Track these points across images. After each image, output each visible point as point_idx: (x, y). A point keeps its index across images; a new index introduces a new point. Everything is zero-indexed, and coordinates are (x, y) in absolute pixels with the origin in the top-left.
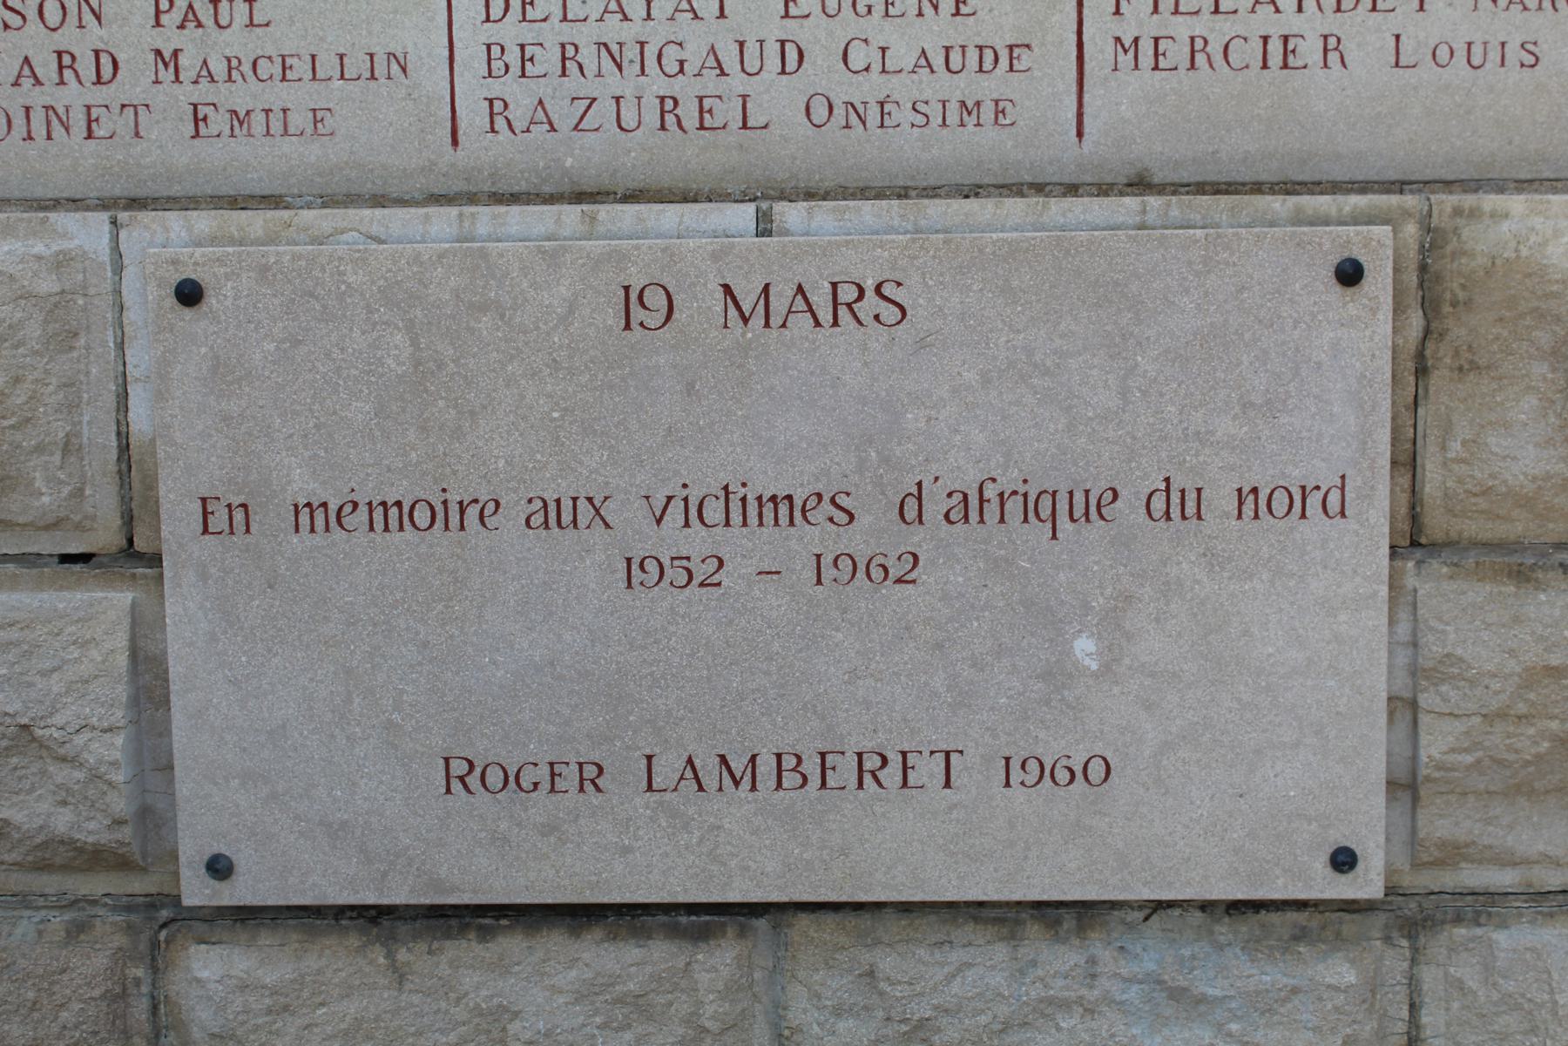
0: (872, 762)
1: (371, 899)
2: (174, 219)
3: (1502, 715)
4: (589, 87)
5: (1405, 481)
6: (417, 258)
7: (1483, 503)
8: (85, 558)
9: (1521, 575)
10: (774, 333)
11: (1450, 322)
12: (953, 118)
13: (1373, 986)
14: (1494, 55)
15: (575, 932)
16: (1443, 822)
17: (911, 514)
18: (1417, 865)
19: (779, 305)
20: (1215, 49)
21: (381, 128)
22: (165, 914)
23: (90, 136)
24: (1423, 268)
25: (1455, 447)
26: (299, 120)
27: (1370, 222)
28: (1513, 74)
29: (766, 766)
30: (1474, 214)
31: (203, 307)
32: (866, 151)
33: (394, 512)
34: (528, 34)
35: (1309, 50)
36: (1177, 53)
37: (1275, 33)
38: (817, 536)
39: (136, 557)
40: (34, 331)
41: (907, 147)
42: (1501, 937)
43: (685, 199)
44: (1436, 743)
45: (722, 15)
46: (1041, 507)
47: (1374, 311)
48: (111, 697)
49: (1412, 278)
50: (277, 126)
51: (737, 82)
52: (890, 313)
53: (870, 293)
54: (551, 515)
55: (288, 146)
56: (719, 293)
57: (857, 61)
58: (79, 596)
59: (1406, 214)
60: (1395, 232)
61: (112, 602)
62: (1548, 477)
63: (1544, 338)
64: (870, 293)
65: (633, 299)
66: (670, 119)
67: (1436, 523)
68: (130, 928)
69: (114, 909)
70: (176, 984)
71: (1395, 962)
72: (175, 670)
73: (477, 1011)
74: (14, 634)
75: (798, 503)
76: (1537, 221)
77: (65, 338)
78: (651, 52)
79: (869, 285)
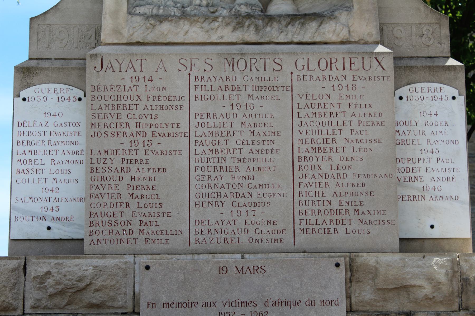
2: (145, 256)
5: (349, 300)
6: (186, 262)
7: (362, 304)
8: (125, 313)
10: (244, 274)
11: (355, 274)
12: (273, 242)
14: (362, 232)
17: (266, 305)
19: (245, 270)
21: (176, 242)
24: (350, 265)
25: (357, 294)
26: (163, 241)
27: (341, 257)
28: (366, 235)
30: (358, 256)
32: (258, 246)
34: (202, 227)
35: (332, 231)
36: (310, 231)
37: (326, 228)
38: (251, 308)
40: (121, 274)
41: (265, 246)
43: (228, 254)
45: (235, 224)
46: (288, 304)
47: (342, 271)
49: (348, 266)
50: (159, 242)
51: (237, 235)
52: (263, 271)
54: (206, 305)
55: (162, 245)
56: (235, 268)
57: (257, 232)
59: (347, 256)
60: (345, 259)
62: (372, 299)
64: (260, 268)
65: (221, 269)
66: (226, 241)
67: (354, 307)
75: (248, 303)
76: (368, 257)
77: (125, 276)
78: (223, 230)
79: (260, 267)
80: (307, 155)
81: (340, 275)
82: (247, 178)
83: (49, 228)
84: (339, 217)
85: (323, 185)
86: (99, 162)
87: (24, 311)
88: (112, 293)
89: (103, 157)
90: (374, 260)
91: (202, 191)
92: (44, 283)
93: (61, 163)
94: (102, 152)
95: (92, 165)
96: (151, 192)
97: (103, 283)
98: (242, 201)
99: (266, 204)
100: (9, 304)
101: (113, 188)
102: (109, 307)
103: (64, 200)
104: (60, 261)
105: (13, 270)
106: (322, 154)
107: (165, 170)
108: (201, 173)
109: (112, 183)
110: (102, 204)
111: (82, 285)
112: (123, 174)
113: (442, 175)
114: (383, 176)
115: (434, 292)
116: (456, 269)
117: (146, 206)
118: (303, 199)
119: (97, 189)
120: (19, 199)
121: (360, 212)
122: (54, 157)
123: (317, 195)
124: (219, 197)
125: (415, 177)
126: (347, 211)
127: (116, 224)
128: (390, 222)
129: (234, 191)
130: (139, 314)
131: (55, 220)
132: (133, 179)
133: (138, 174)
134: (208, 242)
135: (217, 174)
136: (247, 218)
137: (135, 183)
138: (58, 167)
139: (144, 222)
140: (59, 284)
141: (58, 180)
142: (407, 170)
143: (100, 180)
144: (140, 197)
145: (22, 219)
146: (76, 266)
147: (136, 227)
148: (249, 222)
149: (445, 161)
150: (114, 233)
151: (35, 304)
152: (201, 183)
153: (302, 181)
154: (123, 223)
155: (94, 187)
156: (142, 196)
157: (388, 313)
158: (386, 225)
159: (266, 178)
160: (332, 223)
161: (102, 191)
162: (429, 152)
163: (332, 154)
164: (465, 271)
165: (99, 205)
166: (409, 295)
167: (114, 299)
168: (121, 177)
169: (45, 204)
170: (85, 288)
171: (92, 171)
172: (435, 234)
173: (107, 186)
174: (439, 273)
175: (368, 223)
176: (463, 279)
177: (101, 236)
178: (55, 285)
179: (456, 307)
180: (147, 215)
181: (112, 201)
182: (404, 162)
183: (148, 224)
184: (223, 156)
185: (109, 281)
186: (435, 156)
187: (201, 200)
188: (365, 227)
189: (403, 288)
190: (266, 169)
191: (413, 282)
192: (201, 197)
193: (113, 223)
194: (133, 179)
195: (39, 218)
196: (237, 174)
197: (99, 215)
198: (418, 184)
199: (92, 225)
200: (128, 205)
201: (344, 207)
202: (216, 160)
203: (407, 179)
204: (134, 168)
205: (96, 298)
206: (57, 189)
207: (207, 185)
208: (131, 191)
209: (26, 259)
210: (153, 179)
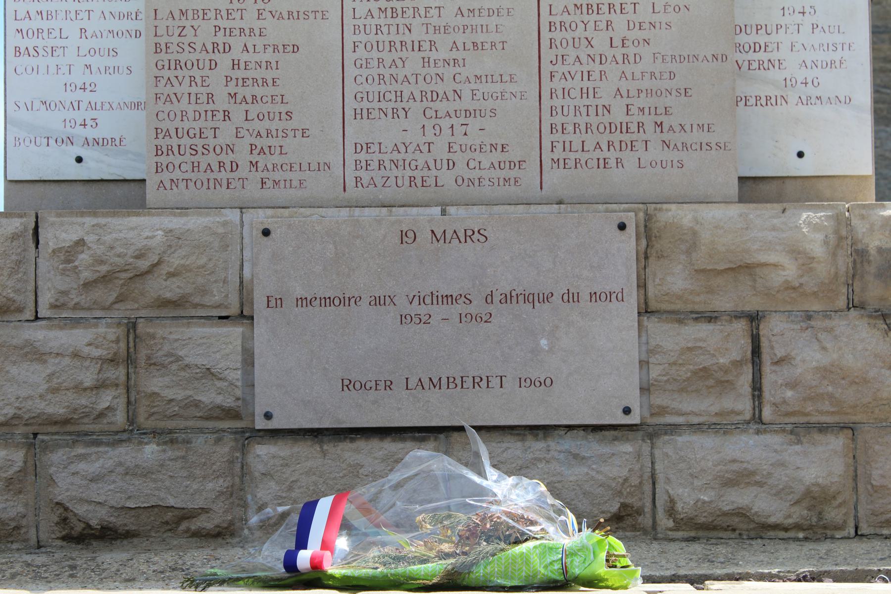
0: (477, 380)
1: (316, 426)
3: (675, 364)
4: (388, 173)
5: (642, 292)
6: (337, 222)
7: (666, 298)
8: (226, 318)
9: (680, 322)
10: (447, 245)
11: (654, 243)
12: (501, 183)
13: (639, 455)
14: (669, 164)
15: (382, 439)
16: (658, 400)
18: (652, 415)
19: (448, 236)
20: (583, 162)
22: (247, 435)
23: (228, 188)
24: (646, 226)
25: (657, 281)
26: (295, 183)
29: (444, 381)
30: (660, 210)
31: (270, 237)
33: (328, 300)
34: (368, 157)
35: (612, 163)
36: (571, 163)
37: (602, 157)
38: (460, 308)
39: (245, 317)
42: (679, 439)
43: (417, 206)
44: (655, 372)
45: (429, 151)
46: (529, 298)
47: (630, 238)
48: (236, 360)
49: (642, 229)
50: (288, 185)
51: (434, 172)
52: (482, 239)
53: (476, 233)
54: (377, 301)
57: (472, 165)
58: (225, 330)
59: (640, 210)
60: (636, 215)
61: (235, 332)
62: (686, 290)
63: (683, 247)
64: (476, 233)
65: (403, 235)
66: (413, 183)
67: (653, 305)
68: (236, 440)
69: (231, 433)
70: (250, 458)
71: (646, 448)
72: (256, 351)
73: (350, 465)
74: (205, 341)
75: (454, 297)
76: (680, 212)
79: (476, 230)
80: (566, 18)
81: (627, 246)
82: (452, 63)
83: (79, 160)
84: (626, 138)
85: (596, 75)
86: (170, 34)
87: (37, 312)
88: (200, 280)
89: (177, 23)
90: (690, 217)
91: (368, 88)
92: (73, 261)
93: (99, 35)
94: (177, 14)
95: (158, 40)
96: (270, 90)
97: (182, 262)
98: (442, 107)
99: (489, 113)
100: (9, 299)
101: (199, 84)
102: (196, 306)
103: (107, 106)
104: (102, 221)
105: (14, 237)
106: (595, 17)
107: (296, 48)
108: (365, 55)
109: (195, 72)
110: (179, 114)
111: (144, 264)
112: (216, 56)
113: (822, 56)
114: (710, 58)
115: (802, 276)
116: (844, 233)
117: (261, 117)
118: (558, 102)
119: (169, 86)
120: (21, 105)
121: (666, 127)
122: (85, 24)
123: (585, 95)
124: (399, 99)
125: (770, 60)
126: (640, 125)
127: (206, 152)
128: (722, 145)
129: (428, 88)
130: (252, 318)
131: (91, 144)
132: (235, 65)
133: (245, 57)
134: (379, 185)
135: (395, 55)
136: (452, 139)
137: (240, 74)
138: (94, 43)
139: (259, 147)
140: (102, 262)
141: (94, 69)
142: (756, 48)
143: (173, 67)
144: (249, 100)
145: (27, 142)
146: (132, 229)
147: (243, 156)
148: (456, 148)
149: (827, 29)
150: (202, 168)
151: (57, 300)
152: (365, 72)
153: (556, 68)
154: (218, 150)
155: (163, 82)
156: (254, 97)
157: (716, 314)
158: (713, 152)
159: (487, 63)
160: (611, 148)
161: (177, 89)
162: (796, 12)
163: (613, 17)
164: (860, 236)
165: (172, 115)
166: (755, 281)
167: (203, 291)
168: (213, 63)
169: (71, 114)
170: (148, 272)
171: (159, 50)
172: (804, 168)
173: (187, 80)
174: (812, 241)
175: (680, 148)
176: (857, 251)
177: (177, 174)
178: (93, 265)
179: (842, 302)
180: (264, 134)
181: (198, 107)
182: (748, 31)
183: (267, 150)
184: (407, 22)
185: (194, 257)
186: (808, 20)
187: (365, 105)
188: (674, 156)
189: (745, 269)
190: (487, 46)
191: (763, 258)
192: (365, 99)
193: (200, 149)
194: (235, 65)
195: (59, 140)
196: (434, 55)
197: (173, 133)
198: (775, 74)
199: (160, 152)
200: (227, 115)
201: (637, 118)
202: (393, 29)
203: (755, 65)
204: (237, 43)
205: (171, 289)
206: (93, 85)
207: (377, 78)
208: (232, 89)
209: (37, 217)
210: (274, 65)
